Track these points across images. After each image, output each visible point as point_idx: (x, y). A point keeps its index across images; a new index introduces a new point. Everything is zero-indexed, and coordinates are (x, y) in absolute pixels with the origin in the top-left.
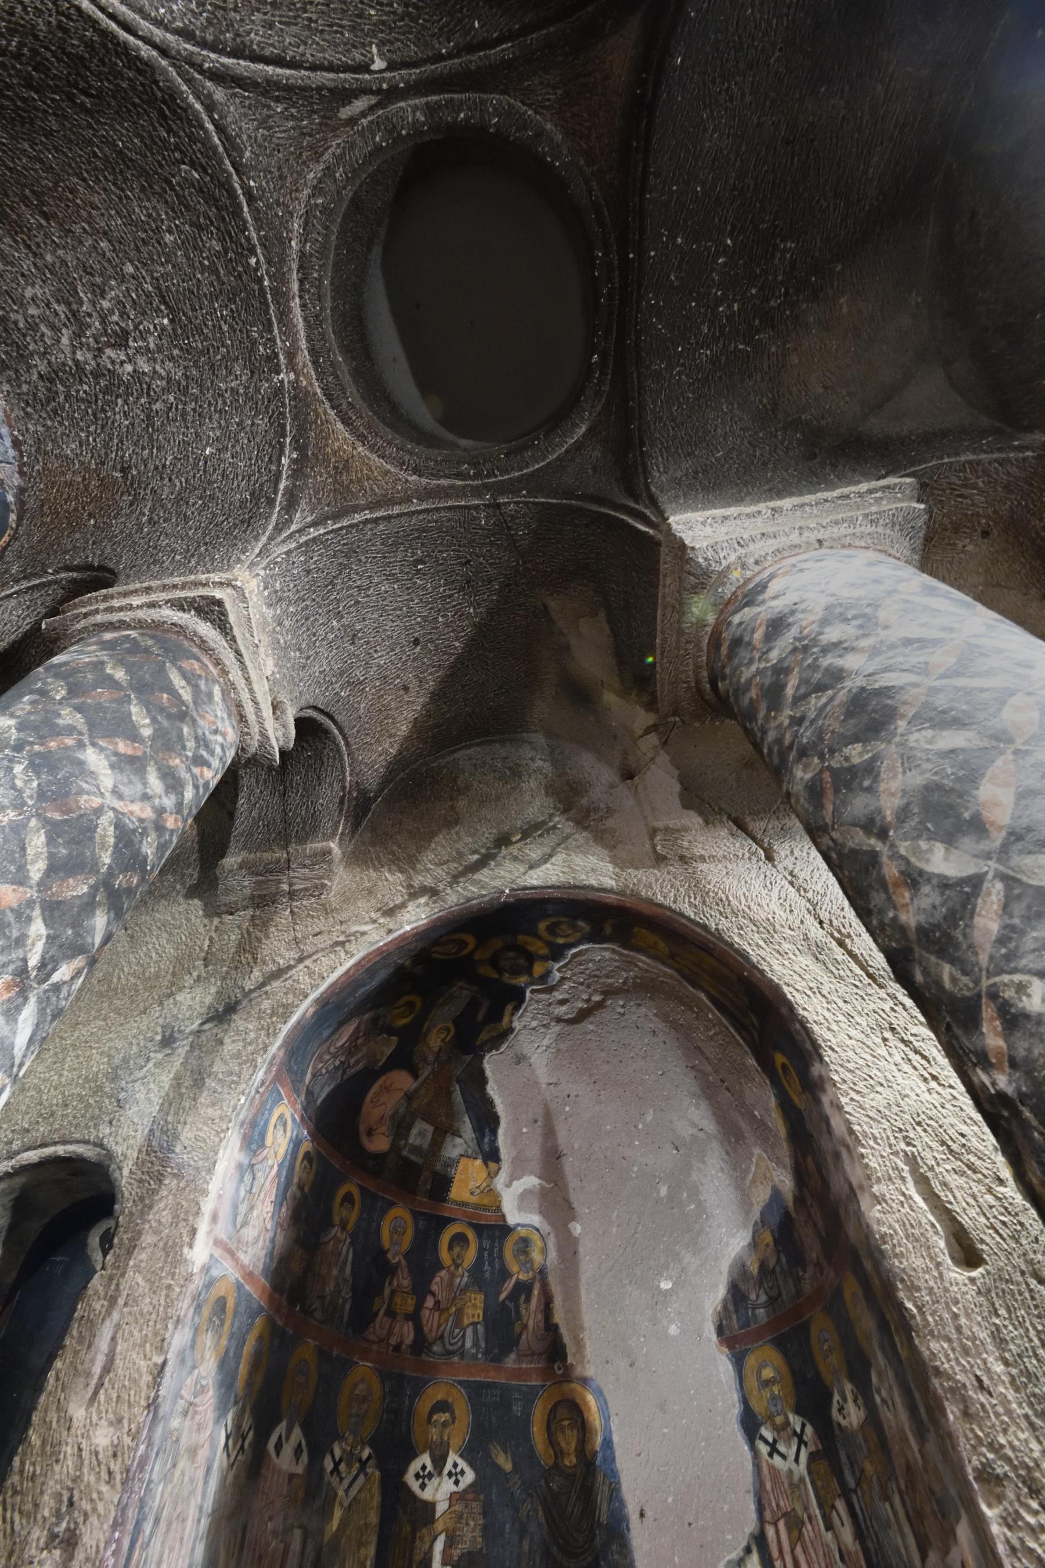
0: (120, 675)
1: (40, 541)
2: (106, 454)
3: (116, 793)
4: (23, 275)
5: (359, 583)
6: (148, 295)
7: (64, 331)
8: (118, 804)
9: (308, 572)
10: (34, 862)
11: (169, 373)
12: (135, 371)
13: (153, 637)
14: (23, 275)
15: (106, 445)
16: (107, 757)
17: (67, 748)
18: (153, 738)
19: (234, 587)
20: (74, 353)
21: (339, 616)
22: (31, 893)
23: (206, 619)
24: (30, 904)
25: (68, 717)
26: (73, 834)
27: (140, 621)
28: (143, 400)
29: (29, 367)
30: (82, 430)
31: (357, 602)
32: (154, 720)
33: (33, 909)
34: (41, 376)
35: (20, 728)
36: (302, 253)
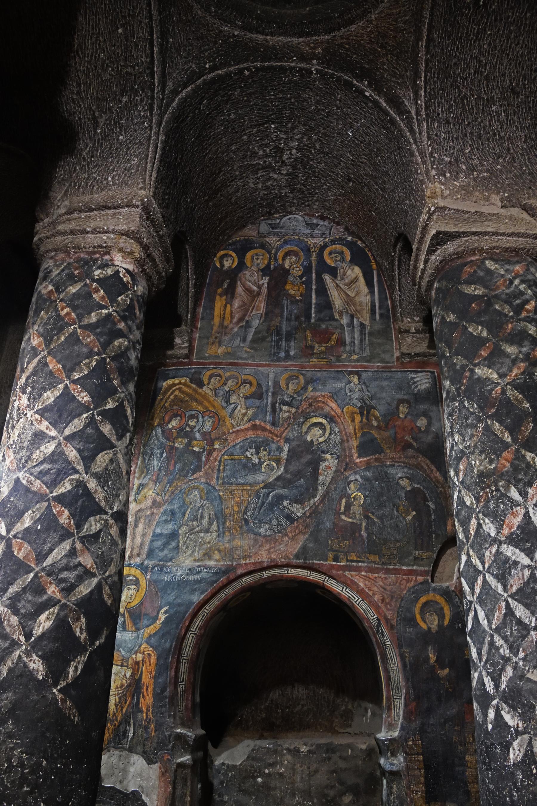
3: (502, 376)
4: (244, 186)
5: (472, 71)
6: (258, 131)
7: (271, 175)
8: (507, 380)
9: (448, 122)
10: (504, 436)
11: (300, 133)
12: (296, 149)
14: (244, 186)
15: (334, 180)
16: (484, 365)
18: (490, 332)
19: (434, 212)
20: (282, 174)
21: (491, 101)
22: (514, 448)
23: (445, 243)
24: (518, 451)
26: (505, 411)
29: (285, 195)
30: (322, 186)
31: (487, 78)
32: (481, 323)
33: (521, 452)
34: (291, 193)
36: (242, 28)
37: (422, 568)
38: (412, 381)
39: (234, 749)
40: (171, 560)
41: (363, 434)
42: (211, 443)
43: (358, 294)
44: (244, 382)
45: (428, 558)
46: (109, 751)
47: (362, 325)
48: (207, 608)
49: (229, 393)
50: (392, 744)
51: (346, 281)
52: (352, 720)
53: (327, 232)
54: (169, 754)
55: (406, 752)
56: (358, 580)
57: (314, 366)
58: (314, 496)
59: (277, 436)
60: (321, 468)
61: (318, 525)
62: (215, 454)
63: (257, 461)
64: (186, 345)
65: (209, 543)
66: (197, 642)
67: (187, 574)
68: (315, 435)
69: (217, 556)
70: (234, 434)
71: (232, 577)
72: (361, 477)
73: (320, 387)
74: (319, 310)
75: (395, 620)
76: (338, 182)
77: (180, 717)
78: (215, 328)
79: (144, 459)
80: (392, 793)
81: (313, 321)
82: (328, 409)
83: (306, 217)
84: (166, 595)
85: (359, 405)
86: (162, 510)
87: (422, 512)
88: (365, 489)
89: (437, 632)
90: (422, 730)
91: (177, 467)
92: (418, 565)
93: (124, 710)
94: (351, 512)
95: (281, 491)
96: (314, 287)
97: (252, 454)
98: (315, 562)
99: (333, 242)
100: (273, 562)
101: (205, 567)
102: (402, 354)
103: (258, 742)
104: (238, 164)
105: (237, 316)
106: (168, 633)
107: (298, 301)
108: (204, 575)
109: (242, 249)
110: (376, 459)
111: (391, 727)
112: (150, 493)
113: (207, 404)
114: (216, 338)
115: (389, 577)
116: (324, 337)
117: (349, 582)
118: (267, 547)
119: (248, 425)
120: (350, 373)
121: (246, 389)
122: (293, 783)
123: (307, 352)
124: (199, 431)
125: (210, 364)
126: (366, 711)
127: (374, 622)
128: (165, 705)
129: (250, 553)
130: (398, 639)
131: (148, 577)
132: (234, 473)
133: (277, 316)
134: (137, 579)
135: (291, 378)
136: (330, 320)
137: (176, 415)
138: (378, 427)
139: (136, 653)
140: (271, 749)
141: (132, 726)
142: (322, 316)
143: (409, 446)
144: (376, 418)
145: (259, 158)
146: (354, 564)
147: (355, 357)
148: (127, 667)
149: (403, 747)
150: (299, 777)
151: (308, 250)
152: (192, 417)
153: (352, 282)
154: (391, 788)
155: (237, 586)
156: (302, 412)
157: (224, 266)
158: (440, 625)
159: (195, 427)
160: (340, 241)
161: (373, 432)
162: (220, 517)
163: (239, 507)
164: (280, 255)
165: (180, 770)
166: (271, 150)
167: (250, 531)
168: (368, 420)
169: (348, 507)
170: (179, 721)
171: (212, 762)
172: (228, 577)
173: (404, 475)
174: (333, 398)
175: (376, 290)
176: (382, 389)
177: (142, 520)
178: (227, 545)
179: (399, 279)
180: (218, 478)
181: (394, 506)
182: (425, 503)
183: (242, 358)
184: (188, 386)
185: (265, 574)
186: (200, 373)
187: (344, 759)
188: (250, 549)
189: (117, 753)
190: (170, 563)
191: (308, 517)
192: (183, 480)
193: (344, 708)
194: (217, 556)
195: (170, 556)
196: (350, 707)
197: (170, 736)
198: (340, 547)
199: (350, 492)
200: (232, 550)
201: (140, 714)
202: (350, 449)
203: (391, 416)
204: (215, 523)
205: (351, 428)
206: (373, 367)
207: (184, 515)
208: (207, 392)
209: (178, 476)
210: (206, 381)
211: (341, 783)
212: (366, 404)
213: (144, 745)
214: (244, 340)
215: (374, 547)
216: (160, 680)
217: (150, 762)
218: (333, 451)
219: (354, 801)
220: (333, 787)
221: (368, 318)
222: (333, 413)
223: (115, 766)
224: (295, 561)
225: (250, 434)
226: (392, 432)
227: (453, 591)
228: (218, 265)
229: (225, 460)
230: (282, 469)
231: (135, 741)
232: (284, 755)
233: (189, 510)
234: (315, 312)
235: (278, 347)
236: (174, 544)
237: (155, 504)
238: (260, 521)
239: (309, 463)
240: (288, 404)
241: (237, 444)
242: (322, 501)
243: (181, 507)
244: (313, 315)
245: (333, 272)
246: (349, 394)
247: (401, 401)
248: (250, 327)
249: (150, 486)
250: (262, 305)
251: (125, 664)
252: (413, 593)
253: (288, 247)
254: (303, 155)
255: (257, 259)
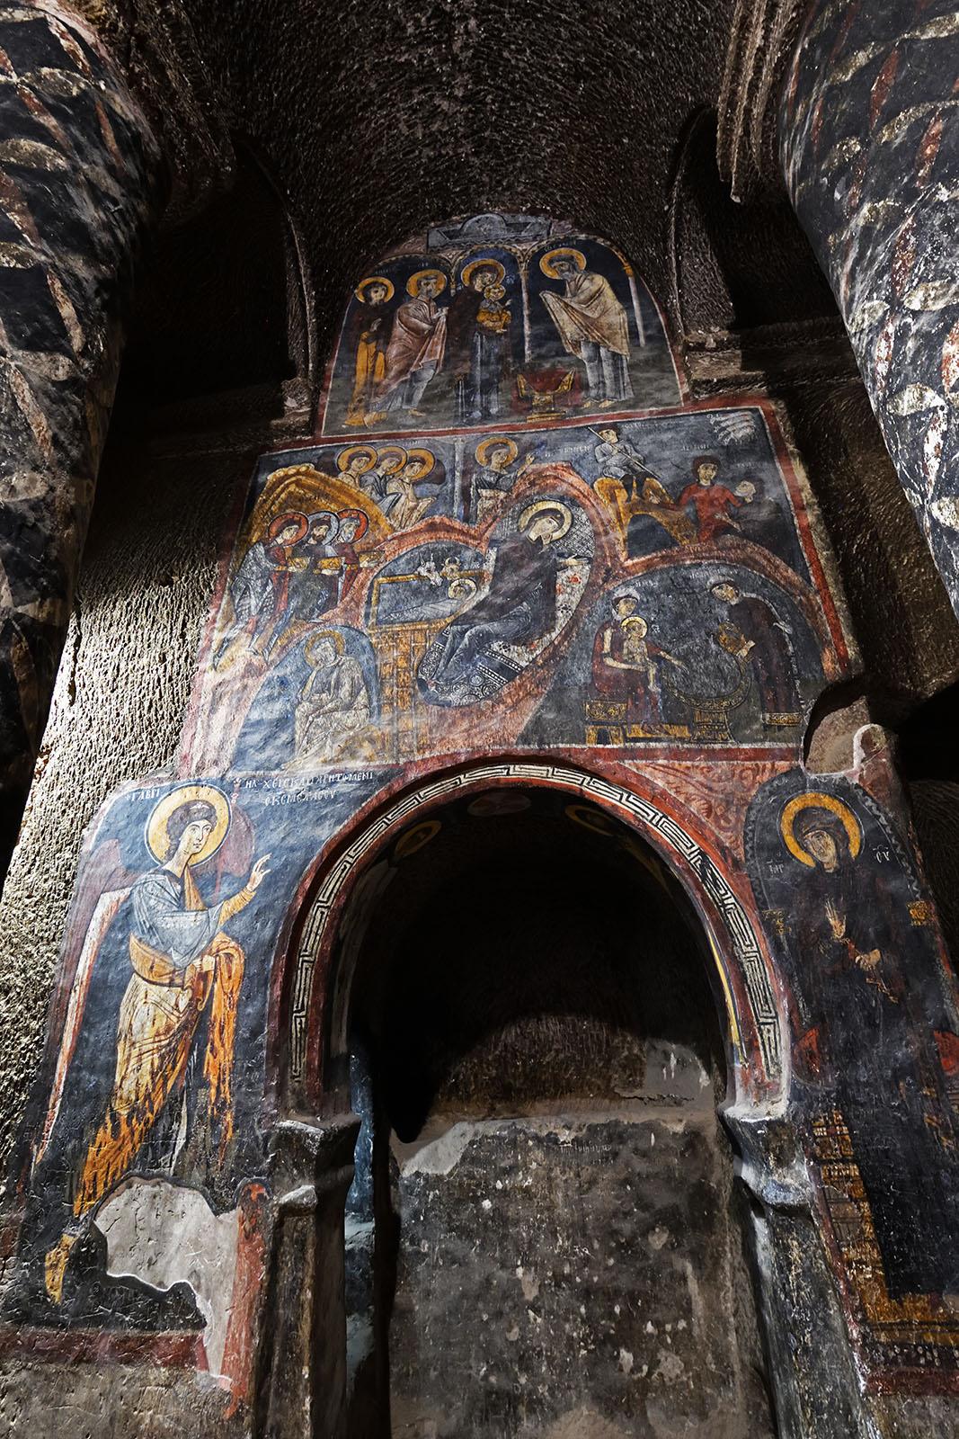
0: (861, 58)
1: (631, 218)
2: (558, 97)
7: (437, 102)
12: (476, 16)
13: (821, 10)
14: (389, 127)
15: (549, 93)
17: (945, 132)
20: (456, 98)
25: (895, 134)
27: (787, 33)
28: (507, 16)
30: (529, 123)
34: (476, 154)
35: (879, 194)
37: (784, 746)
38: (717, 428)
39: (438, 1142)
40: (278, 766)
41: (635, 520)
42: (354, 559)
43: (604, 312)
44: (411, 461)
45: (794, 724)
46: (130, 1186)
47: (616, 357)
48: (352, 853)
49: (385, 479)
50: (776, 1134)
51: (582, 297)
52: (642, 1075)
53: (544, 232)
54: (263, 1184)
55: (813, 1157)
56: (651, 773)
57: (534, 426)
58: (550, 629)
59: (474, 538)
60: (559, 581)
61: (562, 678)
62: (361, 576)
63: (439, 580)
64: (305, 409)
65: (352, 728)
66: (330, 924)
67: (310, 789)
68: (544, 529)
69: (367, 750)
70: (396, 542)
71: (397, 787)
72: (638, 590)
73: (548, 454)
74: (538, 341)
75: (741, 850)
76: (558, 97)
77: (294, 1092)
78: (358, 388)
79: (232, 598)
80: (790, 1264)
81: (527, 360)
82: (565, 486)
83: (506, 216)
84: (267, 832)
85: (622, 474)
86: (263, 679)
87: (767, 641)
88: (648, 609)
89: (837, 871)
90: (844, 1098)
91: (293, 604)
92: (773, 740)
93: (170, 1084)
94: (625, 651)
95: (486, 627)
96: (526, 312)
97: (429, 571)
98: (561, 746)
99: (554, 245)
100: (478, 751)
101: (344, 773)
102: (696, 385)
103: (480, 1127)
104: (371, 59)
105: (396, 367)
106: (270, 906)
107: (500, 335)
108: (342, 787)
109: (401, 274)
110: (662, 557)
111: (763, 1090)
112: (243, 652)
113: (347, 500)
114: (360, 401)
115: (717, 766)
116: (550, 381)
117: (634, 781)
118: (465, 725)
119: (422, 524)
120: (602, 427)
121: (416, 471)
122: (551, 1208)
123: (522, 405)
124: (331, 543)
125: (350, 439)
126: (668, 1059)
127: (695, 860)
128: (258, 1067)
129: (431, 739)
130: (754, 890)
131: (234, 801)
132: (397, 603)
133: (464, 361)
134: (212, 807)
135: (494, 446)
136: (557, 355)
137: (290, 522)
138: (662, 506)
139: (201, 955)
140: (504, 1138)
141: (184, 1120)
142: (543, 351)
143: (728, 529)
144: (656, 491)
145: (411, 47)
146: (641, 745)
147: (608, 403)
148: (182, 987)
149: (805, 1141)
150: (560, 1195)
151: (512, 262)
152: (319, 523)
153: (591, 298)
154: (787, 1248)
155: (410, 805)
156: (517, 496)
157: (371, 299)
158: (842, 857)
159: (324, 537)
160: (567, 242)
161: (653, 514)
162: (373, 680)
163: (408, 660)
164: (465, 274)
165: (290, 1221)
166: (428, 20)
167: (430, 700)
168: (640, 495)
169: (617, 644)
170: (291, 1103)
171: (398, 1172)
172: (390, 788)
173: (722, 579)
174: (574, 469)
175: (635, 303)
176: (663, 445)
177: (225, 700)
178: (388, 729)
179: (679, 263)
180: (367, 616)
181: (708, 634)
182: (770, 625)
183: (405, 426)
184: (313, 476)
185: (465, 780)
186: (333, 454)
187: (644, 1154)
188: (431, 731)
189: (147, 1189)
190: (277, 772)
191: (542, 667)
192: (302, 625)
193: (626, 1053)
194: (367, 750)
195: (275, 759)
196: (636, 1051)
197: (266, 1138)
198: (609, 715)
199: (618, 618)
200: (396, 736)
201: (202, 1091)
202: (612, 546)
203: (683, 488)
204: (363, 692)
205: (611, 511)
206: (641, 414)
207: (304, 684)
208: (346, 481)
209: (293, 619)
210: (342, 464)
211: (644, 1207)
212: (634, 471)
213: (208, 1166)
214: (409, 400)
215: (677, 712)
216: (250, 1010)
217: (219, 1207)
218: (580, 552)
219: (672, 1245)
220: (627, 1214)
221: (625, 345)
222: (575, 492)
223: (141, 1224)
224: (521, 749)
225: (424, 539)
226: (688, 509)
227: (857, 786)
228: (361, 299)
229: (379, 584)
230: (486, 591)
231: (189, 1155)
232: (530, 1149)
233: (314, 674)
234: (532, 348)
235: (469, 403)
236: (284, 737)
237: (251, 671)
238: (449, 681)
239: (537, 575)
240: (490, 486)
241: (400, 557)
242: (566, 635)
243: (298, 670)
244: (527, 352)
245: (559, 288)
246: (601, 460)
247: (698, 461)
248: (418, 381)
249: (242, 641)
250: (439, 348)
251: (178, 981)
252: (772, 793)
253: (478, 261)
254: (493, 34)
255: (427, 284)
